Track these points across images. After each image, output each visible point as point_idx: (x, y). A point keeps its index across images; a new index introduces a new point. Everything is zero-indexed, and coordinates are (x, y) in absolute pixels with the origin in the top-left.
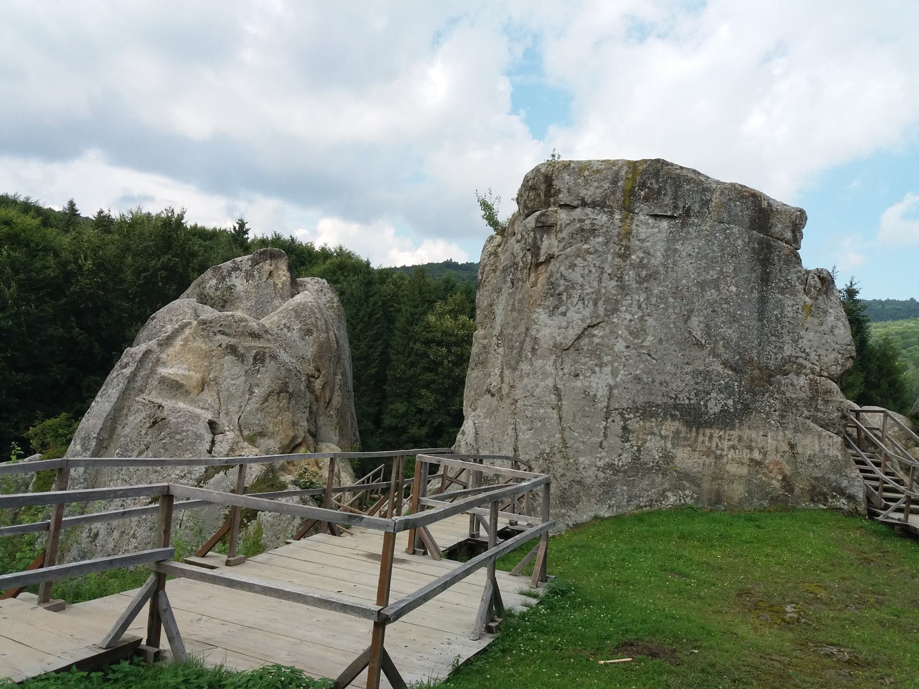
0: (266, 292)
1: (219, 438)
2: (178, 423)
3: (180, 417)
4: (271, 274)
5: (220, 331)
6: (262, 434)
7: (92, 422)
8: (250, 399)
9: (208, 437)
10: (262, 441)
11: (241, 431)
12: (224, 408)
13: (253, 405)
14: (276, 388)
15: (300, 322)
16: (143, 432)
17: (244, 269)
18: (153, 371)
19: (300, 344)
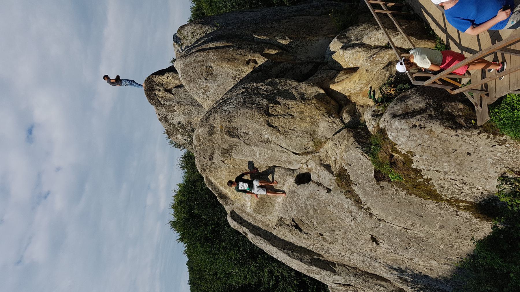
0: (183, 96)
1: (313, 177)
2: (298, 211)
3: (291, 207)
4: (169, 91)
5: (210, 159)
6: (313, 134)
7: (294, 265)
8: (275, 143)
9: (311, 187)
10: (320, 133)
11: (308, 153)
12: (284, 166)
13: (281, 140)
14: (263, 118)
15: (200, 78)
16: (305, 236)
17: (166, 113)
18: (249, 215)
19: (221, 81)
